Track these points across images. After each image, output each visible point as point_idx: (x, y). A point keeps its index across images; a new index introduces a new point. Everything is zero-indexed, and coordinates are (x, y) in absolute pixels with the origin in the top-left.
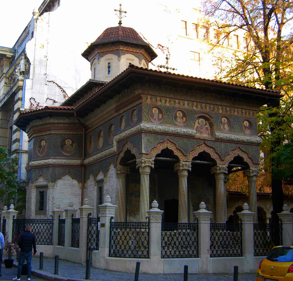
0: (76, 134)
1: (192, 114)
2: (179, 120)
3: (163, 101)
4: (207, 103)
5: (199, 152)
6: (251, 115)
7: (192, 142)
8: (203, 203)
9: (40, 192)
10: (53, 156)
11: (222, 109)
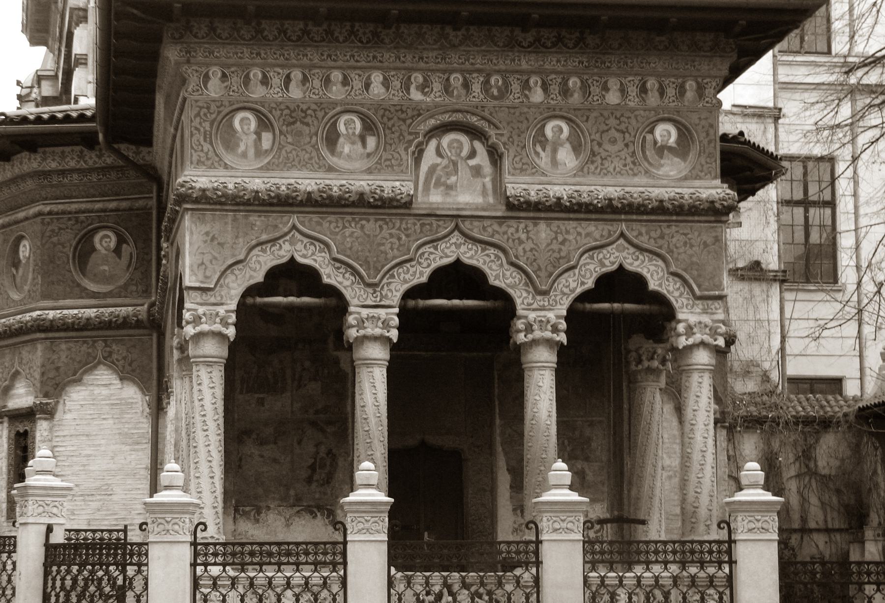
0: (131, 209)
1: (404, 120)
2: (347, 149)
3: (276, 81)
4: (470, 72)
5: (434, 266)
6: (690, 94)
7: (399, 229)
8: (367, 464)
9: (18, 434)
10: (45, 296)
11: (545, 87)
